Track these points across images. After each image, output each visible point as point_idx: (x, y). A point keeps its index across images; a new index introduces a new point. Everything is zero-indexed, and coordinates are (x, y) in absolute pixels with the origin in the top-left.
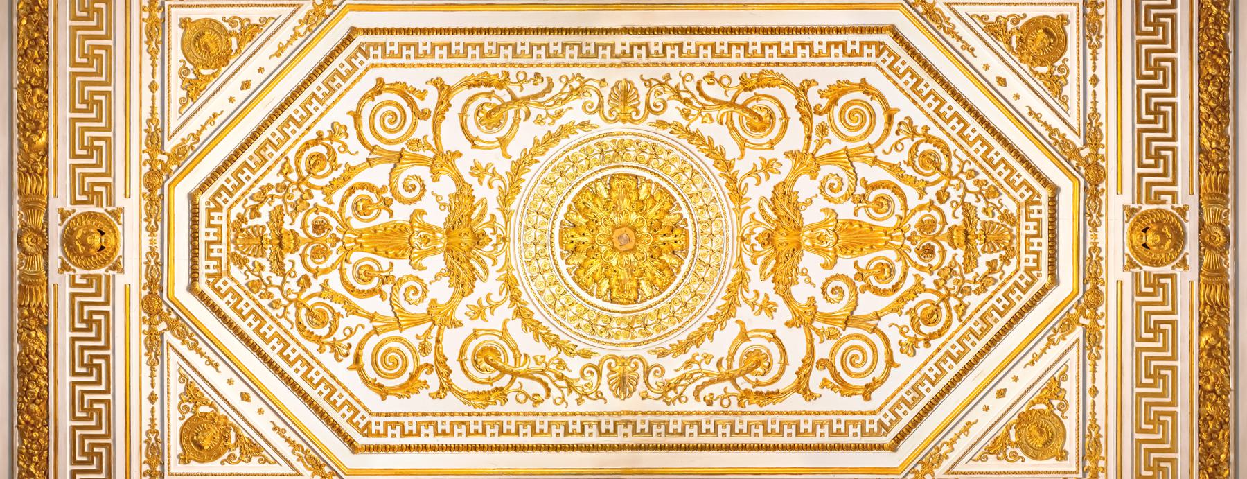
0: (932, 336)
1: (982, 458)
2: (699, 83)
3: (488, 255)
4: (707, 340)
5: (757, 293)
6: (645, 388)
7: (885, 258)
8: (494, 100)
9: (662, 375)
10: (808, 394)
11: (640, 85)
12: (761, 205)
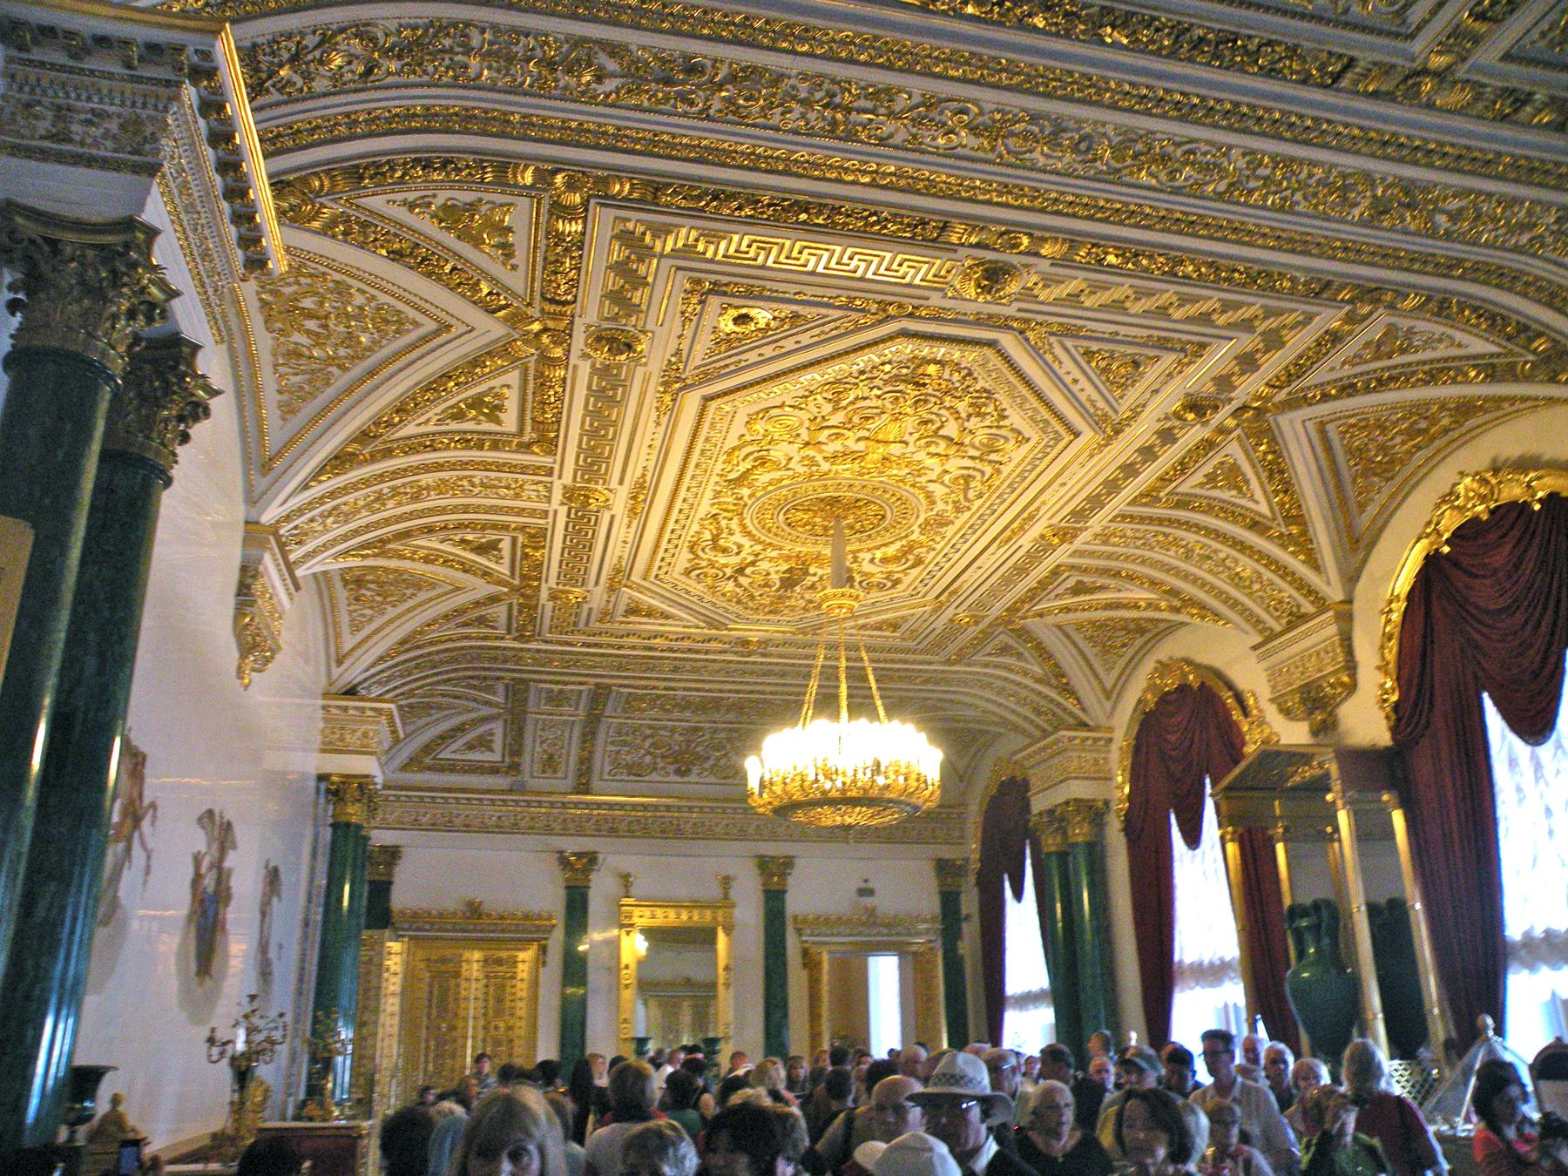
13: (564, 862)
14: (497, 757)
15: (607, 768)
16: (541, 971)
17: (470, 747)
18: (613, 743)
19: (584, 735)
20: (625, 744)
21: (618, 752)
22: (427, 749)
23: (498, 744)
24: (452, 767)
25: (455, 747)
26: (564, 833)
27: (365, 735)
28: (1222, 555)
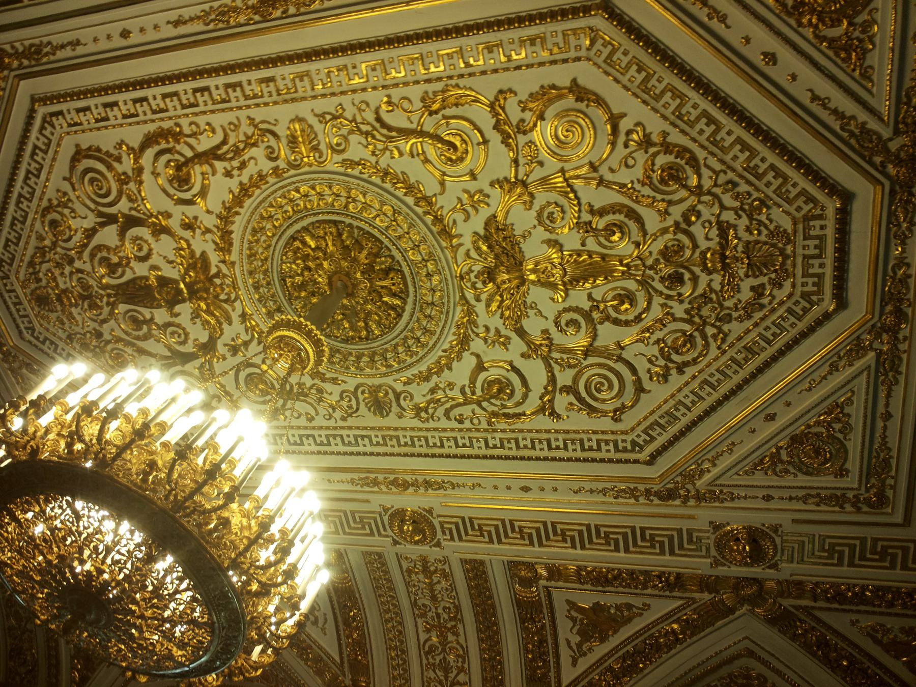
0: (686, 364)
1: (750, 473)
2: (377, 112)
3: (226, 301)
4: (446, 370)
5: (487, 329)
6: (399, 410)
7: (624, 289)
8: (177, 156)
9: (412, 399)
10: (553, 414)
12: (474, 243)
28: (462, 678)
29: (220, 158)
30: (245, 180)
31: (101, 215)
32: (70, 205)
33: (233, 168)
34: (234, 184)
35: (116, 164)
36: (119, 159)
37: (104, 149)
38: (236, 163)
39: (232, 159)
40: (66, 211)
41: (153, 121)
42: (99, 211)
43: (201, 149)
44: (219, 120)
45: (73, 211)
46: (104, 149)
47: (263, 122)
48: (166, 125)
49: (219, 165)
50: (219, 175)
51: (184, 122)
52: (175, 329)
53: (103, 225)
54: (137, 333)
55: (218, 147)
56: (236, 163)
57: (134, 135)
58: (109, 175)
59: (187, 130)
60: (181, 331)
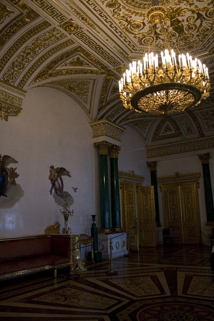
11: (105, 4)
13: (201, 157)
14: (174, 132)
15: (206, 128)
16: (198, 189)
17: (166, 131)
18: (203, 119)
19: (194, 119)
20: (207, 119)
21: (207, 122)
22: (155, 134)
23: (172, 129)
24: (164, 138)
25: (161, 132)
26: (200, 149)
27: (102, 131)
29: (127, 20)
30: (130, 14)
31: (157, 39)
32: (157, 44)
33: (128, 16)
34: (133, 16)
35: (141, 38)
36: (139, 37)
37: (138, 40)
38: (127, 16)
39: (126, 17)
40: (159, 45)
41: (125, 33)
42: (156, 40)
43: (127, 24)
44: (117, 22)
45: (158, 44)
46: (138, 40)
47: (112, 13)
48: (125, 31)
49: (129, 20)
50: (132, 19)
51: (122, 28)
52: (189, 18)
53: (160, 38)
54: (194, 29)
55: (124, 20)
56: (127, 16)
57: (131, 36)
58: (144, 39)
59: (124, 27)
60: (189, 18)
